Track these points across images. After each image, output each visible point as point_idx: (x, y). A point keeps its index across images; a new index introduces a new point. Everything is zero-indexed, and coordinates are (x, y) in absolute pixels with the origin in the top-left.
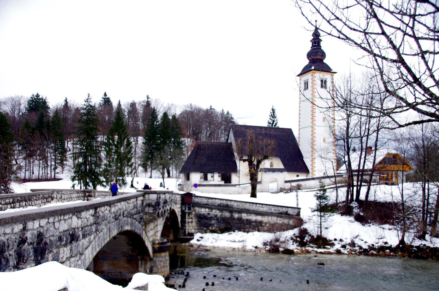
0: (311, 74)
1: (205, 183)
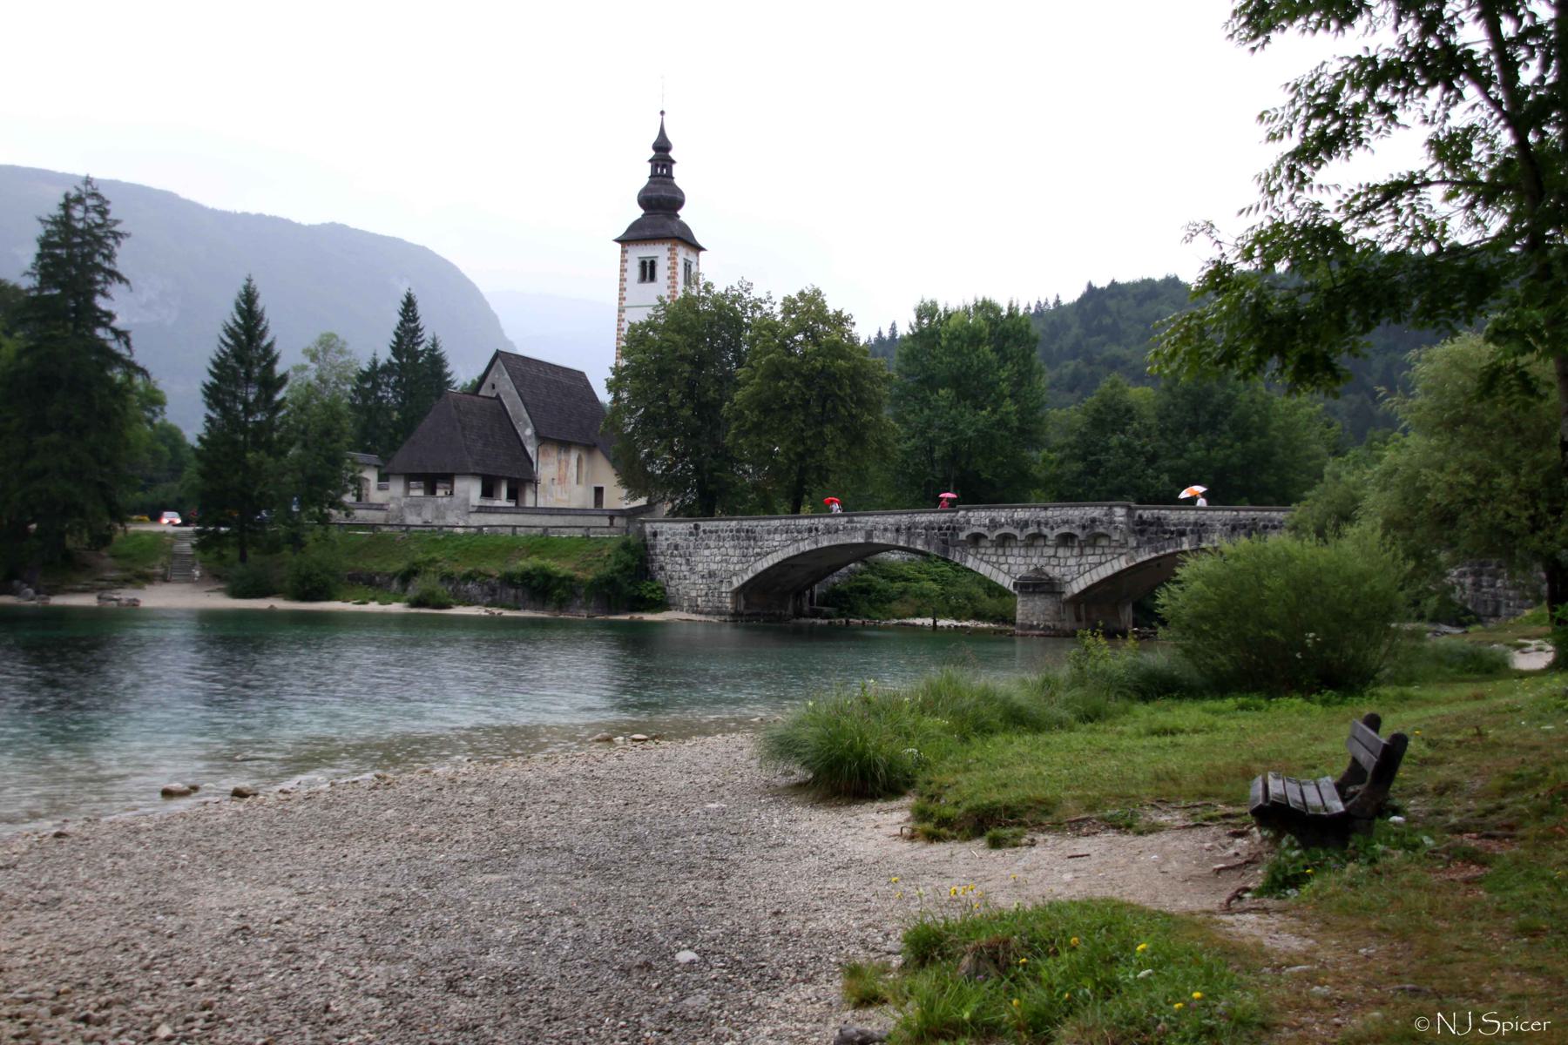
1: (488, 503)
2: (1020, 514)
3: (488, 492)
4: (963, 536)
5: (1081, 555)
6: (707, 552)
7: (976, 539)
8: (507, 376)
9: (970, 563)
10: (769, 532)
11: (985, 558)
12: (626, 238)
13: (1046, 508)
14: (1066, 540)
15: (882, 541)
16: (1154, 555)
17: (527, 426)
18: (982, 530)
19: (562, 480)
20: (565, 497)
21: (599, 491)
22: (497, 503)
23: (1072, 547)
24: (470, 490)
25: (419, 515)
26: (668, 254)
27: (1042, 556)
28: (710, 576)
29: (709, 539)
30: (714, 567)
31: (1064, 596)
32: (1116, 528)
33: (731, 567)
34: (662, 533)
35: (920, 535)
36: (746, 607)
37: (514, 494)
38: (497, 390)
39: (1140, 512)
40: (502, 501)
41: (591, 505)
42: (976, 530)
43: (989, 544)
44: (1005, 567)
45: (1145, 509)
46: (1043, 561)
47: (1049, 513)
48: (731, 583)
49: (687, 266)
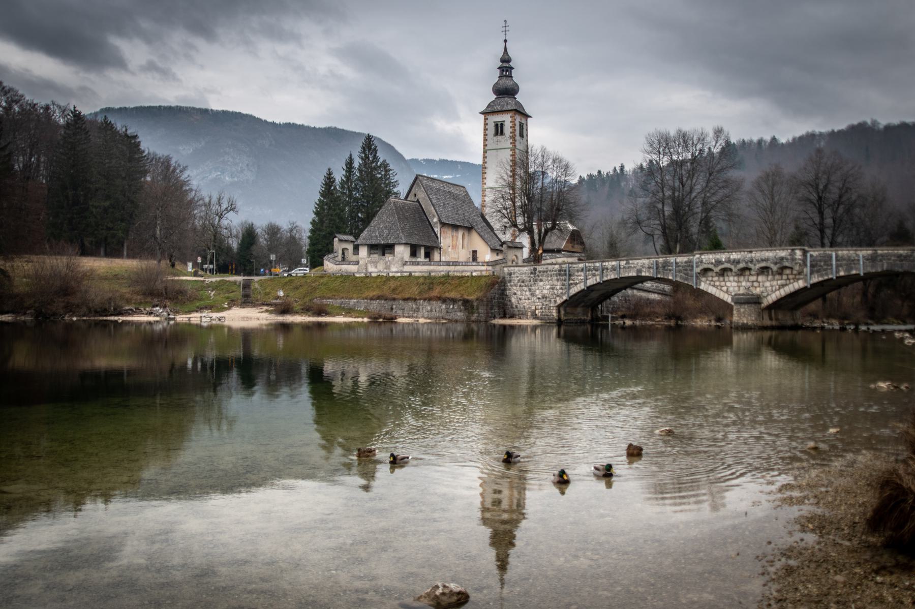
0: (511, 115)
2: (734, 256)
3: (414, 254)
4: (698, 270)
5: (774, 279)
6: (541, 284)
7: (706, 271)
8: (422, 189)
9: (703, 286)
10: (578, 271)
11: (712, 283)
12: (485, 112)
13: (751, 252)
14: (764, 270)
15: (647, 274)
16: (821, 279)
17: (434, 216)
18: (711, 266)
19: (454, 247)
20: (456, 256)
21: (475, 252)
22: (419, 260)
23: (768, 275)
24: (402, 251)
25: (376, 267)
26: (511, 119)
27: (748, 281)
28: (543, 298)
29: (542, 275)
30: (545, 292)
31: (763, 305)
32: (796, 263)
33: (556, 291)
34: (514, 273)
35: (670, 270)
36: (565, 315)
37: (427, 255)
38: (417, 197)
39: (812, 253)
40: (421, 258)
41: (471, 260)
42: (706, 266)
43: (714, 274)
44: (725, 289)
45: (814, 251)
46: (749, 284)
47: (753, 255)
48: (555, 302)
49: (521, 126)
